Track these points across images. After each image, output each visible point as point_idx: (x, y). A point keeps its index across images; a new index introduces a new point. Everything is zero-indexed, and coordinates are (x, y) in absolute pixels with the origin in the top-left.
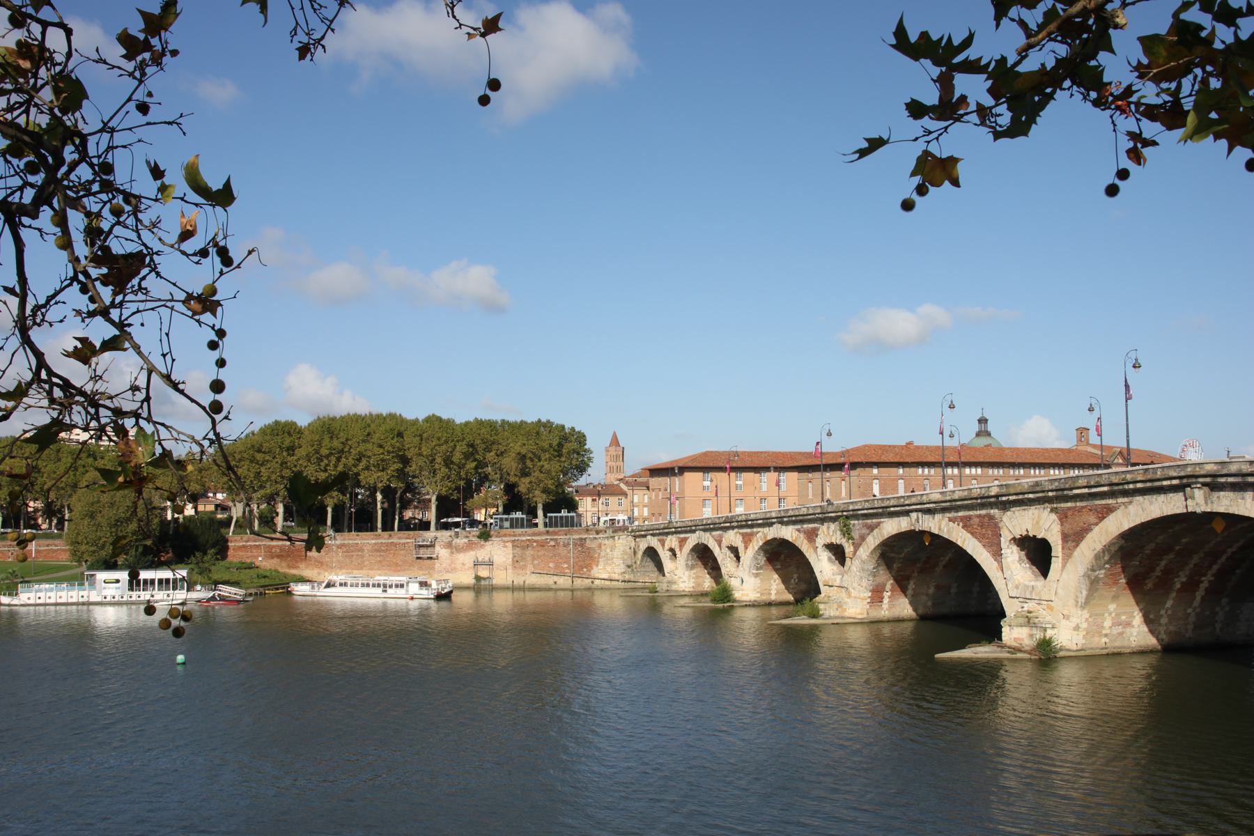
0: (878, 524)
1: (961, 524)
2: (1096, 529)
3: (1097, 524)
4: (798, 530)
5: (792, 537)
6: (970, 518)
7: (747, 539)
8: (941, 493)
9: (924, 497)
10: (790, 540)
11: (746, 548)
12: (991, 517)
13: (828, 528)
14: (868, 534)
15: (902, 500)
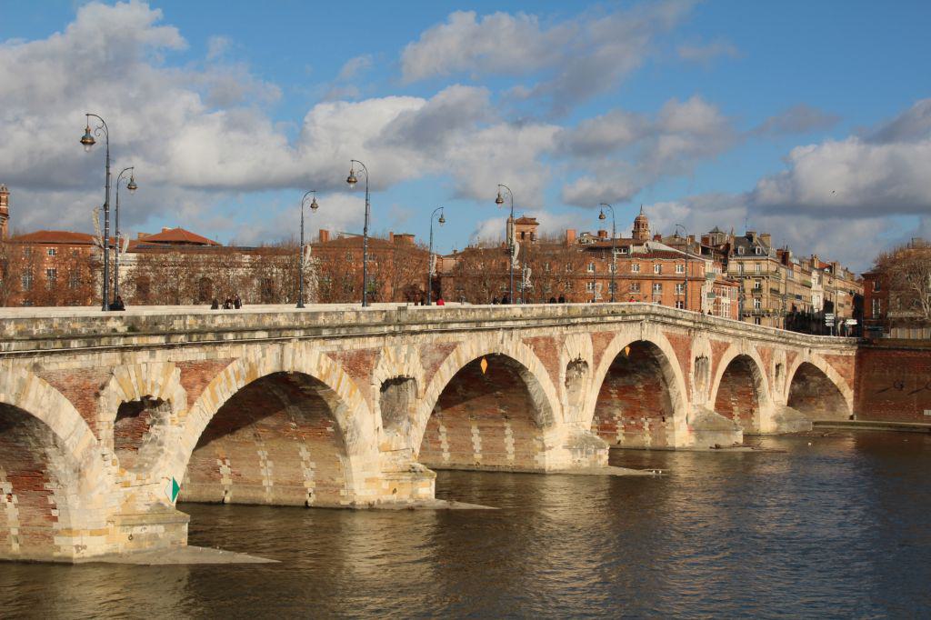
0: (454, 346)
1: (532, 347)
2: (607, 352)
3: (605, 348)
4: (332, 355)
5: (319, 368)
6: (536, 340)
7: (196, 377)
8: (523, 309)
9: (508, 312)
10: (316, 375)
11: (191, 402)
12: (551, 340)
13: (397, 351)
14: (441, 362)
15: (488, 313)
